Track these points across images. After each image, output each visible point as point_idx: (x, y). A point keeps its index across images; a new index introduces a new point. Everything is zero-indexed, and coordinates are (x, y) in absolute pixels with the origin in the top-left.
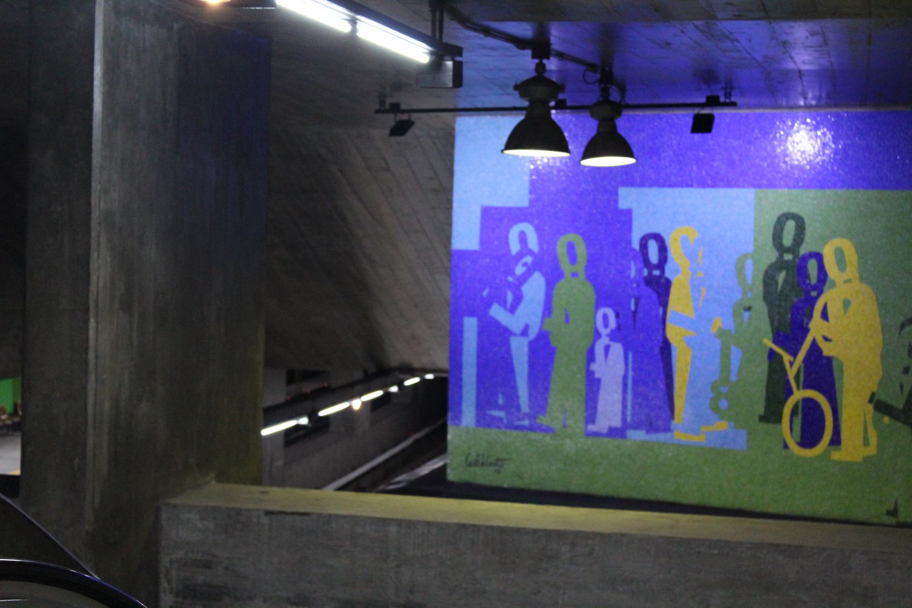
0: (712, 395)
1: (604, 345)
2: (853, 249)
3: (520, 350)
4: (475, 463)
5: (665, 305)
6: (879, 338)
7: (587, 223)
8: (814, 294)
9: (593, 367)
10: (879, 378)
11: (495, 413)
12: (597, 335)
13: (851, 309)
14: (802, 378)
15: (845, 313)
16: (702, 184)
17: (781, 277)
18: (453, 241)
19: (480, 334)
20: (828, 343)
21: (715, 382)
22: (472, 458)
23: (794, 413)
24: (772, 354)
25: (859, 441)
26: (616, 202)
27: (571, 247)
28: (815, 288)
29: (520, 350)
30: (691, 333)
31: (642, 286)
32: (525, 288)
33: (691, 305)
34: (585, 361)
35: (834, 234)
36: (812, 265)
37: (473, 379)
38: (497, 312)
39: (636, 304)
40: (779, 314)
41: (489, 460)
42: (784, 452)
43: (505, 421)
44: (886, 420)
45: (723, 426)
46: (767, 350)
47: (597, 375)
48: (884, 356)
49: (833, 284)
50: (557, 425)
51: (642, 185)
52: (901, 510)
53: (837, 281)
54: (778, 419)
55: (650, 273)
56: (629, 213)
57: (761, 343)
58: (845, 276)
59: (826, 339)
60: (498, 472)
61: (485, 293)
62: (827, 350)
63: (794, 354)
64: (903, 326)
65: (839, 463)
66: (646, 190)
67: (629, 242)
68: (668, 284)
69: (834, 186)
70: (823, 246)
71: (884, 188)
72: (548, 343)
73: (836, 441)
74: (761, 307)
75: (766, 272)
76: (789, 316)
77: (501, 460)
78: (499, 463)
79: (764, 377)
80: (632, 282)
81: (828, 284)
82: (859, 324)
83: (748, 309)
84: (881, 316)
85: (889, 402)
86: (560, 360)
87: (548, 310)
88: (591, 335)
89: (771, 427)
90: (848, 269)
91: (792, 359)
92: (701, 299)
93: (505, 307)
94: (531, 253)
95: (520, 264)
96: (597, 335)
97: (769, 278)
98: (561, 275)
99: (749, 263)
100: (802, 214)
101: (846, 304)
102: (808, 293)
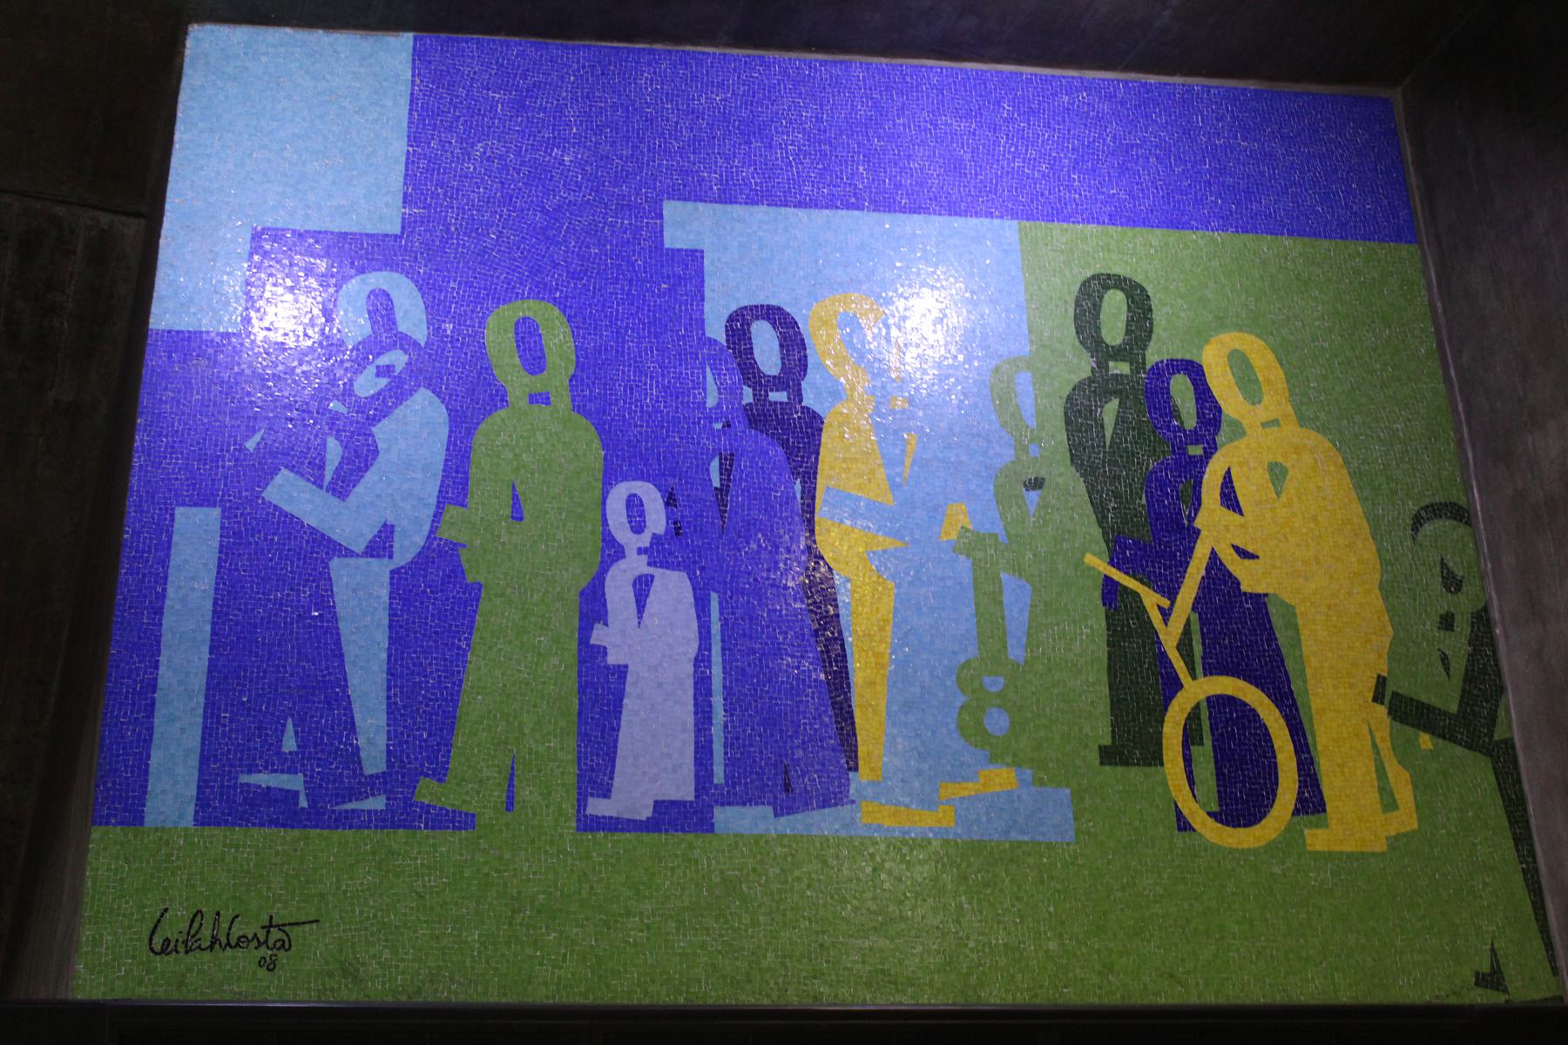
0: (961, 699)
1: (630, 577)
2: (1271, 356)
3: (362, 602)
4: (190, 943)
5: (809, 477)
6: (1368, 550)
7: (573, 276)
8: (1196, 450)
9: (599, 636)
10: (1387, 641)
11: (263, 779)
12: (612, 551)
13: (1290, 486)
14: (1198, 649)
15: (1278, 494)
16: (885, 203)
17: (1110, 412)
18: (155, 309)
19: (225, 553)
20: (1247, 562)
21: (968, 662)
22: (175, 927)
23: (1190, 737)
24: (1110, 586)
25: (1372, 798)
26: (659, 234)
27: (527, 334)
28: (1195, 437)
29: (362, 602)
30: (885, 542)
31: (739, 427)
32: (382, 431)
33: (881, 474)
35: (1221, 324)
36: (1181, 389)
37: (199, 681)
38: (288, 492)
39: (725, 471)
40: (1117, 496)
41: (236, 932)
42: (1181, 839)
43: (303, 803)
44: (1426, 741)
45: (1002, 778)
46: (1100, 581)
47: (612, 659)
48: (1388, 590)
49: (1238, 431)
50: (483, 802)
51: (726, 198)
52: (1510, 970)
53: (1245, 422)
54: (1154, 757)
55: (760, 398)
56: (696, 256)
57: (1079, 564)
58: (1263, 412)
59: (1244, 554)
60: (270, 966)
61: (250, 445)
62: (1249, 578)
63: (1171, 592)
64: (1417, 522)
65: (1329, 856)
66: (737, 210)
67: (701, 323)
68: (813, 424)
69: (1205, 225)
70: (1200, 348)
71: (1315, 234)
72: (457, 572)
73: (1311, 802)
74: (1068, 481)
75: (1069, 398)
76: (1144, 501)
77: (280, 927)
78: (275, 939)
79: (1103, 652)
80: (710, 419)
81: (1225, 427)
82: (1315, 519)
83: (1036, 484)
84: (1363, 500)
85: (1424, 698)
86: (491, 615)
87: (455, 483)
88: (592, 551)
89: (1135, 774)
90: (1266, 398)
91: (1166, 603)
92: (908, 462)
93: (318, 482)
94: (404, 342)
95: (371, 370)
96: (612, 551)
97: (1078, 415)
98: (499, 398)
99: (1024, 381)
100: (1139, 279)
101: (1277, 473)
102: (1180, 450)
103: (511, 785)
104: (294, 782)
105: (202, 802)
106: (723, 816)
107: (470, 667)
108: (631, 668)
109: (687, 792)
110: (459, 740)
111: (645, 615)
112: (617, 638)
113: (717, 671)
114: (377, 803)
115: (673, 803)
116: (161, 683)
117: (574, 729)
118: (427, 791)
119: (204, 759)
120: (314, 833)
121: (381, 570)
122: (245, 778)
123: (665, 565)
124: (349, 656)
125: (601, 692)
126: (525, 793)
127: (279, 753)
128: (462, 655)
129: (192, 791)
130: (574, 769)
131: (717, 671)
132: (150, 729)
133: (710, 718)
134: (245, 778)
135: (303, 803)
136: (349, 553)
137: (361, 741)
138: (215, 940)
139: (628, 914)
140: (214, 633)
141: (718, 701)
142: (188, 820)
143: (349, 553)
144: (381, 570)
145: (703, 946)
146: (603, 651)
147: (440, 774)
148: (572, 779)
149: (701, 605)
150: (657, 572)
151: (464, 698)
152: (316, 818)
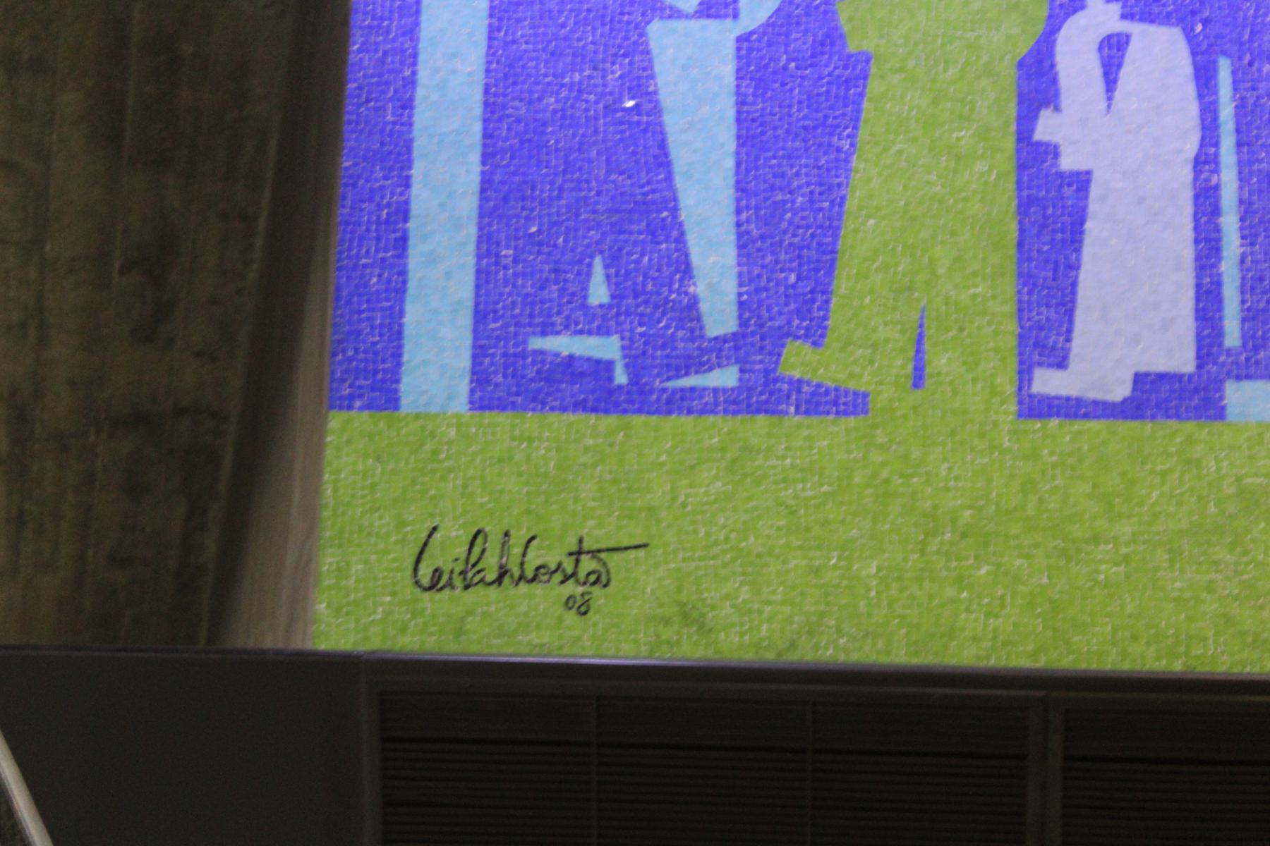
9: (1047, 127)
22: (448, 553)
34: (1012, 109)
37: (468, 204)
41: (532, 561)
43: (621, 378)
47: (1068, 163)
50: (880, 376)
72: (833, 37)
77: (594, 553)
78: (586, 571)
103: (919, 350)
104: (607, 348)
105: (480, 378)
106: (1237, 395)
107: (856, 178)
108: (1096, 177)
109: (1182, 360)
110: (842, 285)
111: (1118, 94)
112: (1073, 132)
113: (1228, 179)
114: (726, 377)
115: (1162, 377)
116: (415, 208)
117: (1011, 268)
118: (798, 360)
119: (481, 316)
120: (638, 420)
121: (721, 37)
122: (536, 343)
123: (1148, 17)
124: (679, 168)
125: (1051, 212)
126: (939, 361)
127: (584, 306)
128: (842, 162)
129: (465, 361)
130: (1012, 327)
131: (1228, 179)
132: (403, 273)
133: (1218, 250)
134: (536, 343)
135: (621, 378)
136: (676, 14)
137: (700, 288)
138: (503, 573)
139: (1096, 539)
140: (487, 135)
141: (1230, 222)
142: (460, 403)
143: (676, 14)
144: (721, 37)
145: (1210, 588)
146: (1053, 151)
147: (815, 334)
148: (1012, 342)
149: (1204, 77)
150: (1136, 29)
151: (848, 225)
152: (638, 399)
